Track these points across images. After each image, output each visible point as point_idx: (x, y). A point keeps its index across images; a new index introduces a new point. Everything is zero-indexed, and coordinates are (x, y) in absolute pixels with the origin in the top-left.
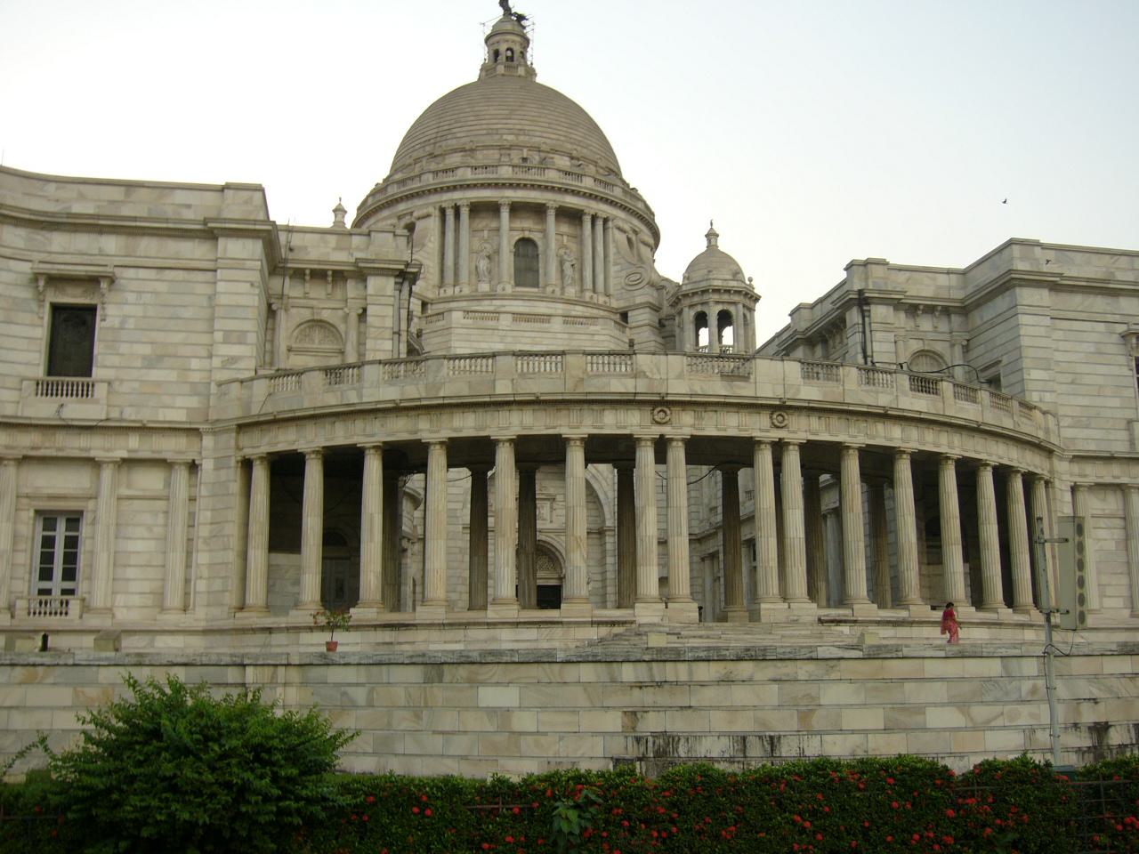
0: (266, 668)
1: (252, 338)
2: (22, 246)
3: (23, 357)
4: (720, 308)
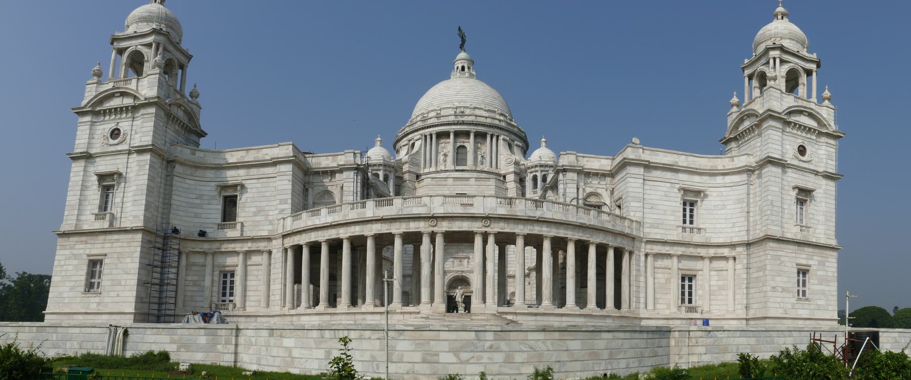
2: (213, 177)
3: (214, 216)
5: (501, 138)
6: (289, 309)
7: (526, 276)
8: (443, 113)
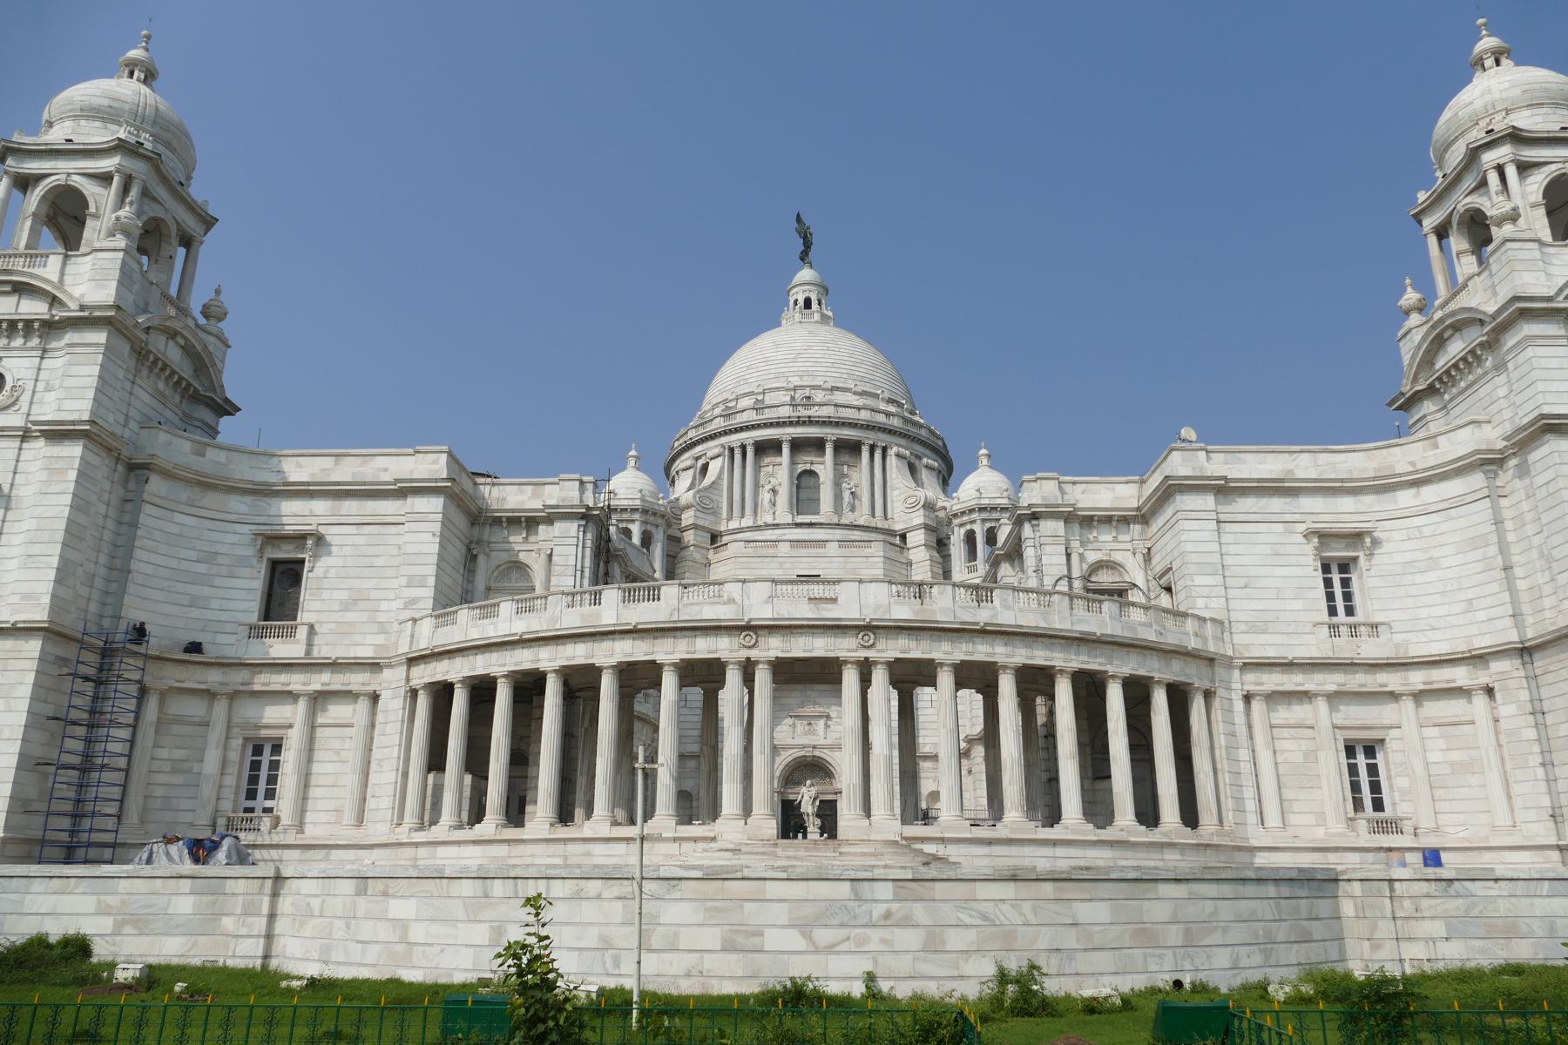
0: (256, 881)
1: (432, 581)
4: (988, 525)
5: (892, 452)
6: (410, 829)
7: (964, 754)
8: (769, 399)
